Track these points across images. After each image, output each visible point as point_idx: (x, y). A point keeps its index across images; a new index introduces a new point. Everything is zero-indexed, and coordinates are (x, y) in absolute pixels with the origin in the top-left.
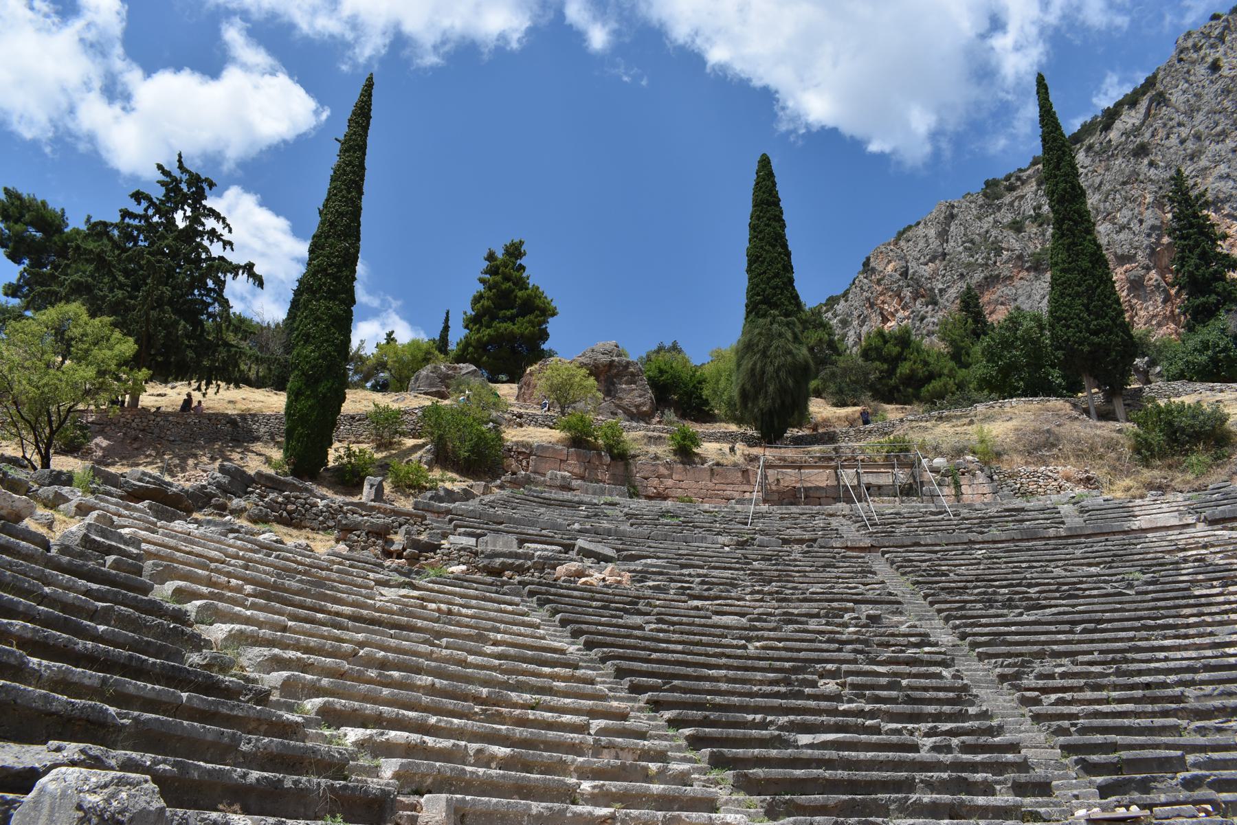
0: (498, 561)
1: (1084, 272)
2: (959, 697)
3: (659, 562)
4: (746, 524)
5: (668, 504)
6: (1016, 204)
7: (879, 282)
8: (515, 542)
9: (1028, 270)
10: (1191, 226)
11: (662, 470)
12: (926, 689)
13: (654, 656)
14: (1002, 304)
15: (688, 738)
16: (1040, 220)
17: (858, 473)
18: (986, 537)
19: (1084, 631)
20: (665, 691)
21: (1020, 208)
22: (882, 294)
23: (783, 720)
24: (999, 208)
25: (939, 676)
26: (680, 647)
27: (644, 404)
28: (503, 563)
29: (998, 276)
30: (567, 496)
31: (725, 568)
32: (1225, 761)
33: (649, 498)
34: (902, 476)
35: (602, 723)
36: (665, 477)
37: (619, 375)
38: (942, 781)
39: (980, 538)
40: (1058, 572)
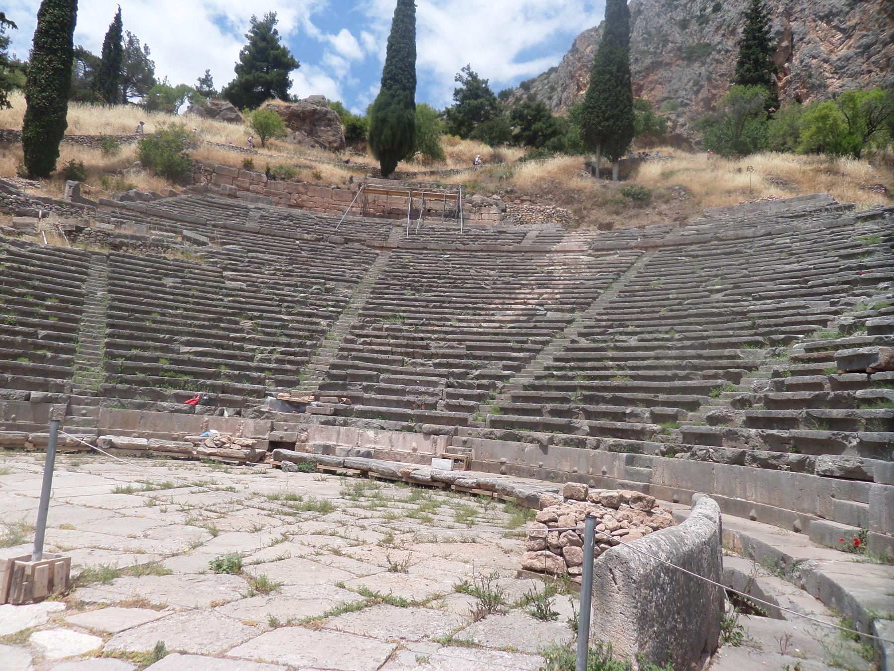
0: (119, 240)
1: (611, 73)
2: (312, 336)
3: (237, 248)
4: (335, 227)
5: (297, 212)
6: (689, 5)
7: (579, 59)
8: (145, 229)
9: (683, 59)
10: (755, 39)
11: (301, 189)
12: (300, 330)
13: (145, 300)
14: (660, 84)
15: (107, 343)
16: (702, 20)
17: (424, 201)
18: (467, 247)
19: (434, 307)
20: (131, 320)
21: (691, 8)
22: (580, 69)
23: (184, 338)
24: (676, 7)
25: (318, 324)
26: (171, 297)
27: (335, 141)
28: (121, 242)
29: (661, 62)
30: (230, 201)
31: (278, 254)
32: (397, 379)
33: (291, 206)
34: (451, 204)
35: (44, 332)
36: (302, 193)
37: (319, 119)
38: (235, 375)
39: (462, 247)
40: (472, 272)
